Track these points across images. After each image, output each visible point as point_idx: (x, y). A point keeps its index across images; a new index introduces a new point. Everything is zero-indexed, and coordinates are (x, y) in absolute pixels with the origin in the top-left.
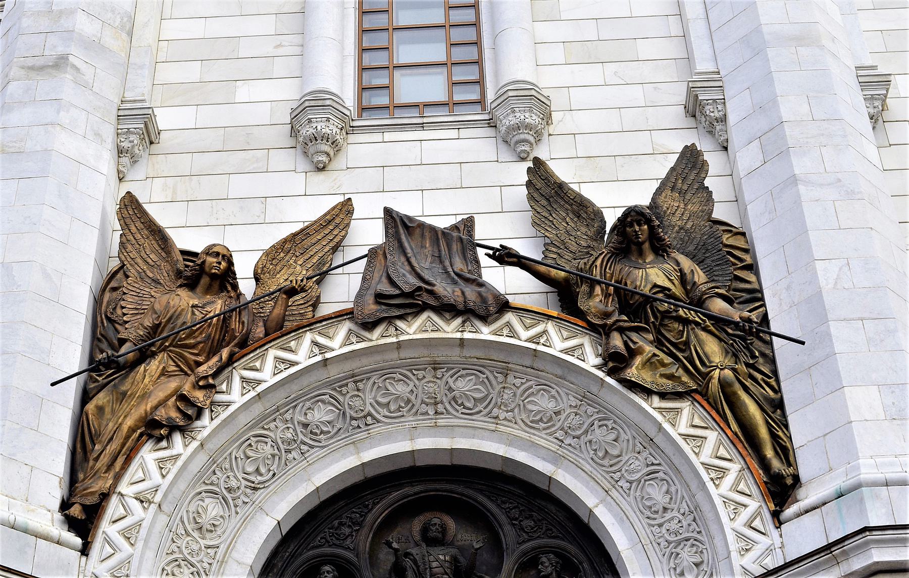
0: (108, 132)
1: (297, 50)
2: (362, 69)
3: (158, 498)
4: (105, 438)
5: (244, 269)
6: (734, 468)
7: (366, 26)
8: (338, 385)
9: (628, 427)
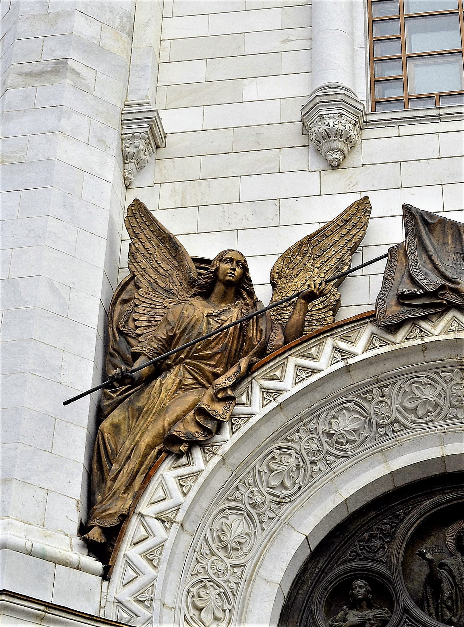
0: (112, 138)
1: (305, 44)
2: (374, 61)
3: (180, 518)
4: (122, 457)
5: (259, 275)
7: (376, 16)
8: (363, 392)
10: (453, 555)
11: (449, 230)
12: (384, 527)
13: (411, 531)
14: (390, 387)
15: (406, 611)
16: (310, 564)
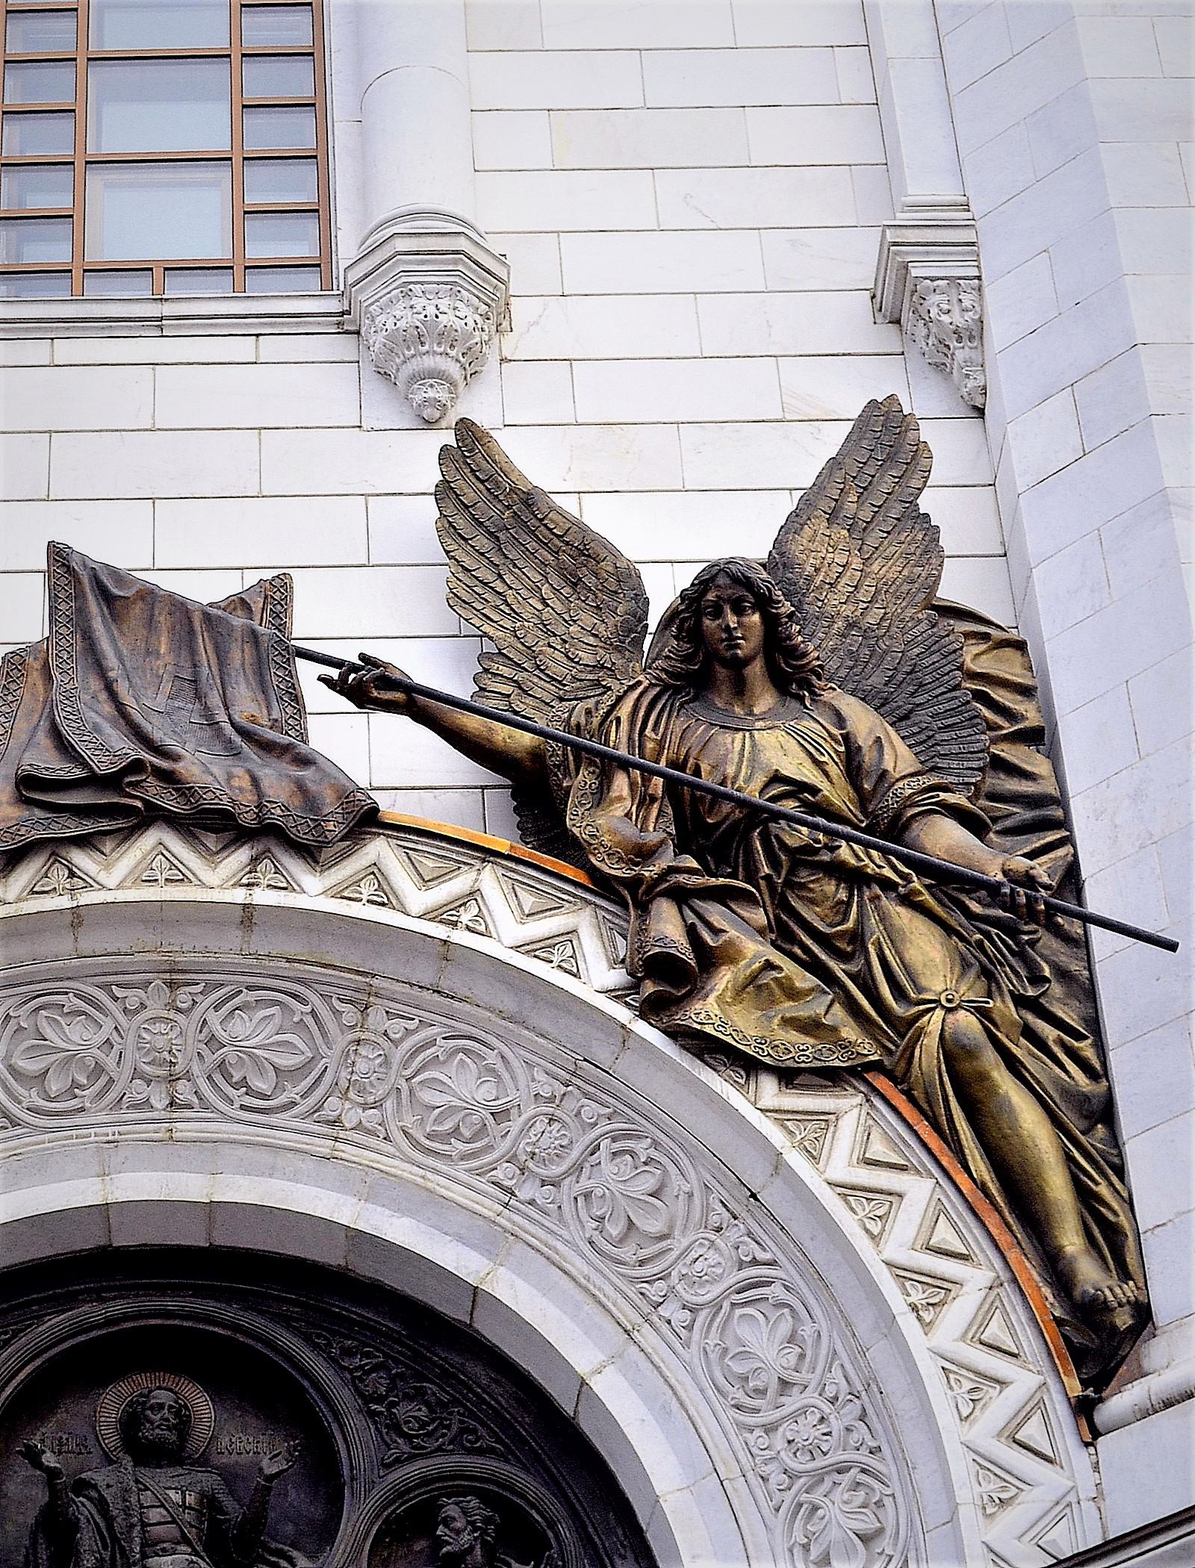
6: (976, 1279)
9: (691, 1157)
10: (111, 1462)
11: (163, 620)
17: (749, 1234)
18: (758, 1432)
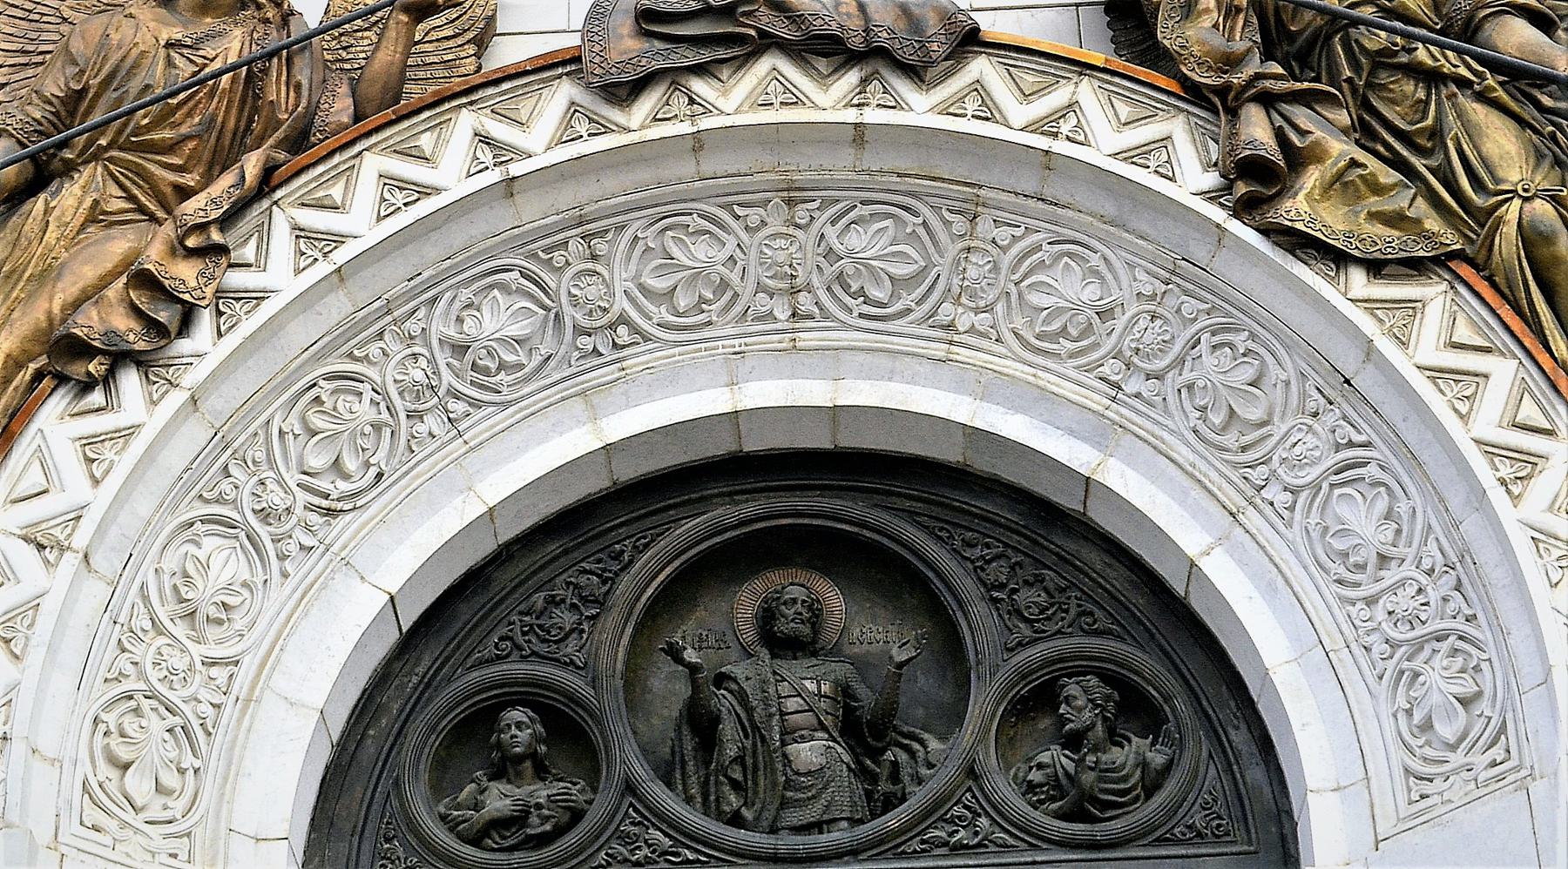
3: (81, 539)
8: (544, 245)
9: (1287, 347)
12: (583, 580)
13: (650, 591)
14: (610, 236)
15: (630, 788)
16: (397, 665)
17: (1345, 418)
18: (1360, 605)
